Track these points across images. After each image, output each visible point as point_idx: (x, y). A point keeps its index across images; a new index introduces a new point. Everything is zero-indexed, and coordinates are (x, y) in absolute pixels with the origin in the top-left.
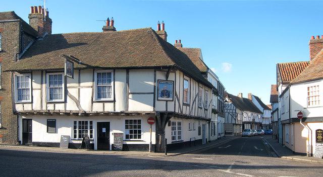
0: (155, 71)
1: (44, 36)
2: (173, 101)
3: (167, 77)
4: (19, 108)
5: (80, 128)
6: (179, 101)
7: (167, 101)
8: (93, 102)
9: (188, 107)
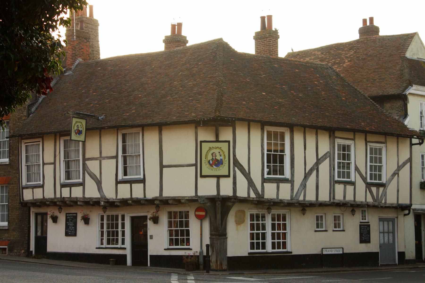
0: (196, 128)
1: (73, 67)
2: (229, 176)
3: (217, 136)
4: (28, 195)
5: (108, 228)
6: (247, 175)
7: (218, 177)
8: (118, 182)
9: (350, 188)
